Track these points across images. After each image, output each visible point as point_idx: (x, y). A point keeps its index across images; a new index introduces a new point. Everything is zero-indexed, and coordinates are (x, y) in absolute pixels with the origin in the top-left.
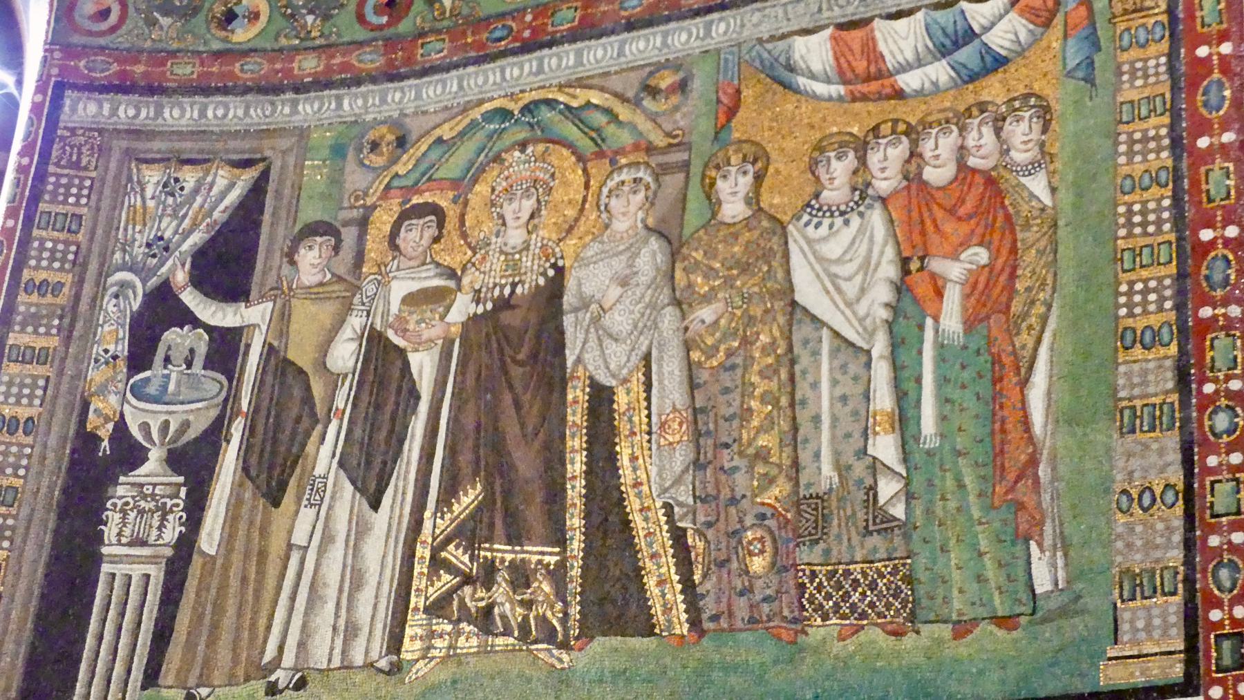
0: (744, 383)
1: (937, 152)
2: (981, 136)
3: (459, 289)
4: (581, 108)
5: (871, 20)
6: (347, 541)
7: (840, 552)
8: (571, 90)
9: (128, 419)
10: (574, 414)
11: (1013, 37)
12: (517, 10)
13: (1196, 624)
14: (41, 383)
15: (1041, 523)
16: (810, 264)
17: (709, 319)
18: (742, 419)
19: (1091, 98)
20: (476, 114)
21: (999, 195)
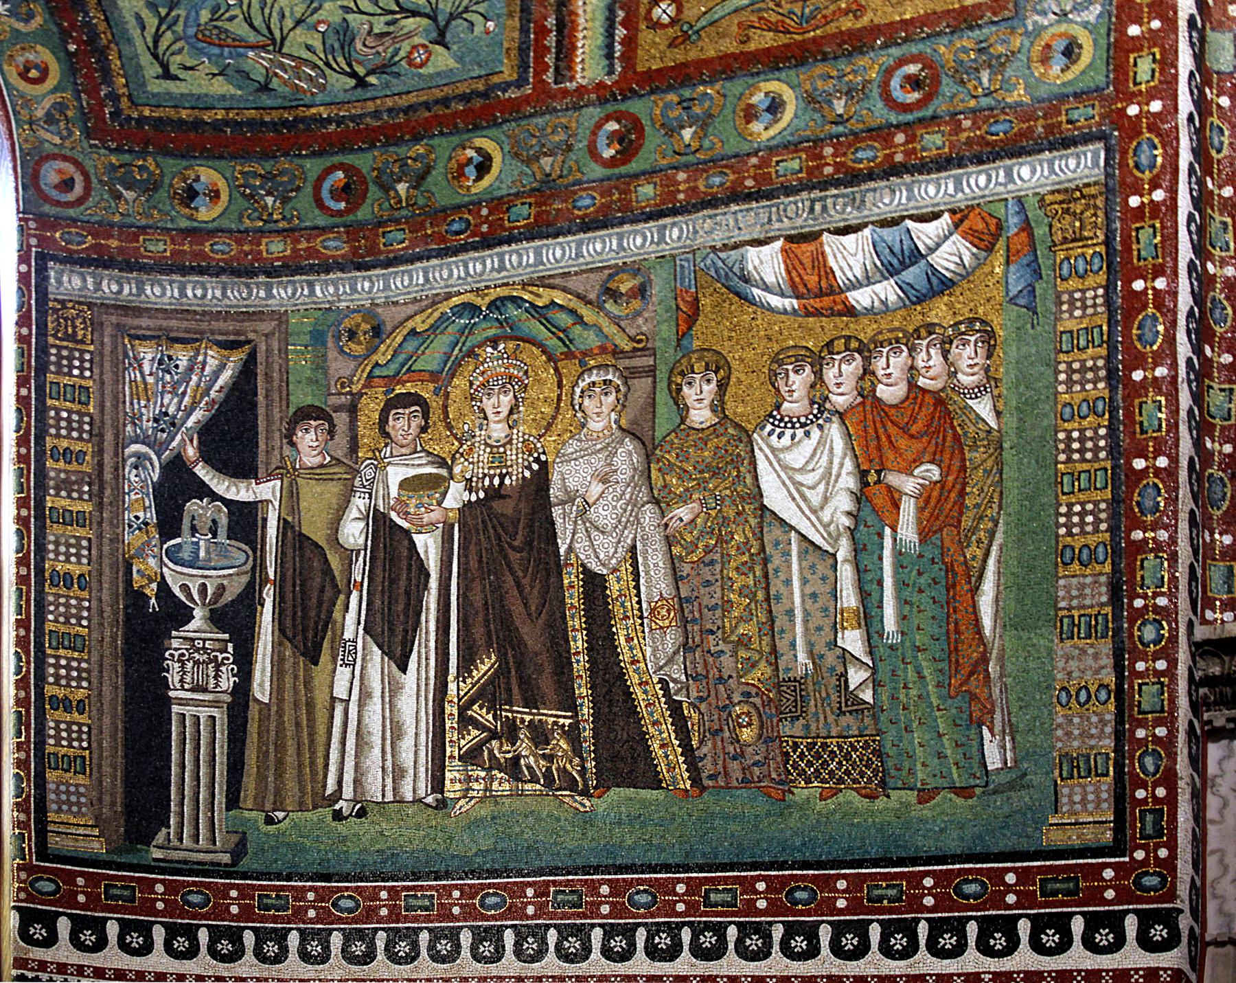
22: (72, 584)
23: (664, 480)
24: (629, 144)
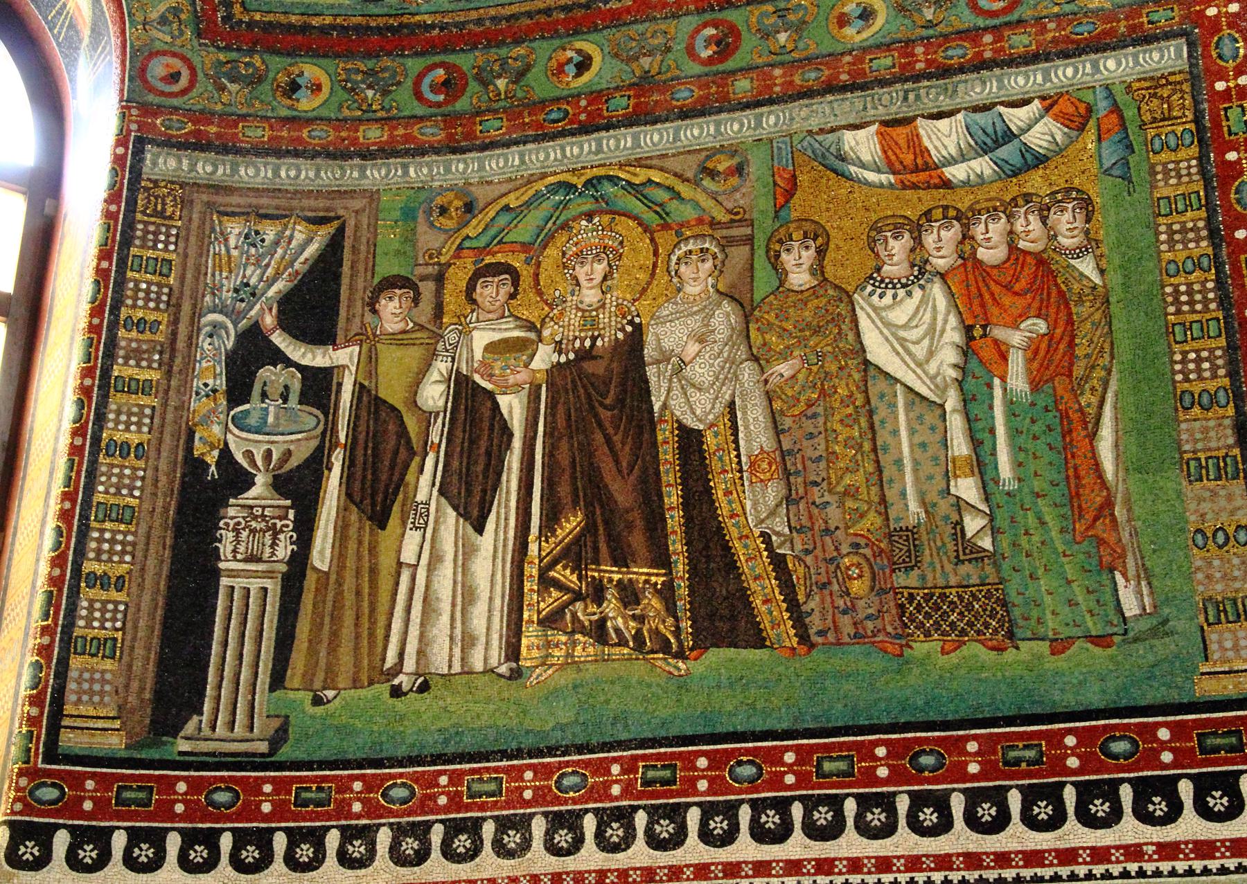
0: (826, 430)
5: (914, 118)
6: (455, 561)
7: (935, 578)
9: (232, 447)
11: (1050, 138)
12: (573, 96)
14: (148, 411)
15: (1123, 556)
16: (878, 328)
17: (787, 374)
18: (828, 461)
19: (1129, 194)
20: (540, 186)
21: (1052, 275)
22: (129, 454)
23: (764, 339)
24: (726, 44)
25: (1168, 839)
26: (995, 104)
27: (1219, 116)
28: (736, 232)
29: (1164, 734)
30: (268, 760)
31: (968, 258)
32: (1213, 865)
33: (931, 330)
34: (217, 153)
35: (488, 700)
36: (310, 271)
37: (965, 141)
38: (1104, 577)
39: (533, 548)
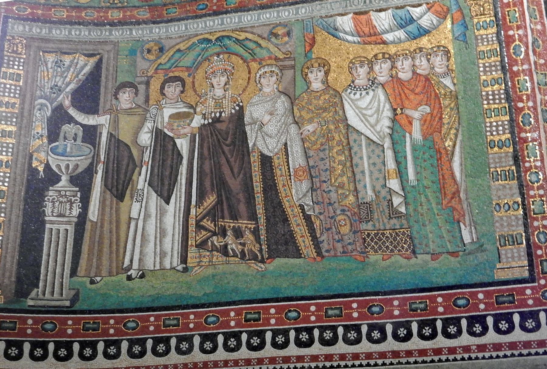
0: (329, 157)
1: (403, 67)
2: (421, 61)
3: (195, 113)
4: (243, 40)
7: (379, 225)
8: (237, 32)
9: (50, 163)
10: (255, 167)
13: (532, 256)
14: (11, 145)
15: (464, 215)
16: (353, 109)
17: (311, 130)
20: (195, 40)
25: (482, 343)
26: (405, 6)
27: (505, 14)
28: (287, 63)
29: (481, 296)
30: (70, 309)
31: (394, 78)
32: (501, 354)
33: (378, 110)
34: (42, 23)
35: (172, 282)
36: (87, 79)
37: (393, 22)
38: (456, 225)
39: (193, 211)
